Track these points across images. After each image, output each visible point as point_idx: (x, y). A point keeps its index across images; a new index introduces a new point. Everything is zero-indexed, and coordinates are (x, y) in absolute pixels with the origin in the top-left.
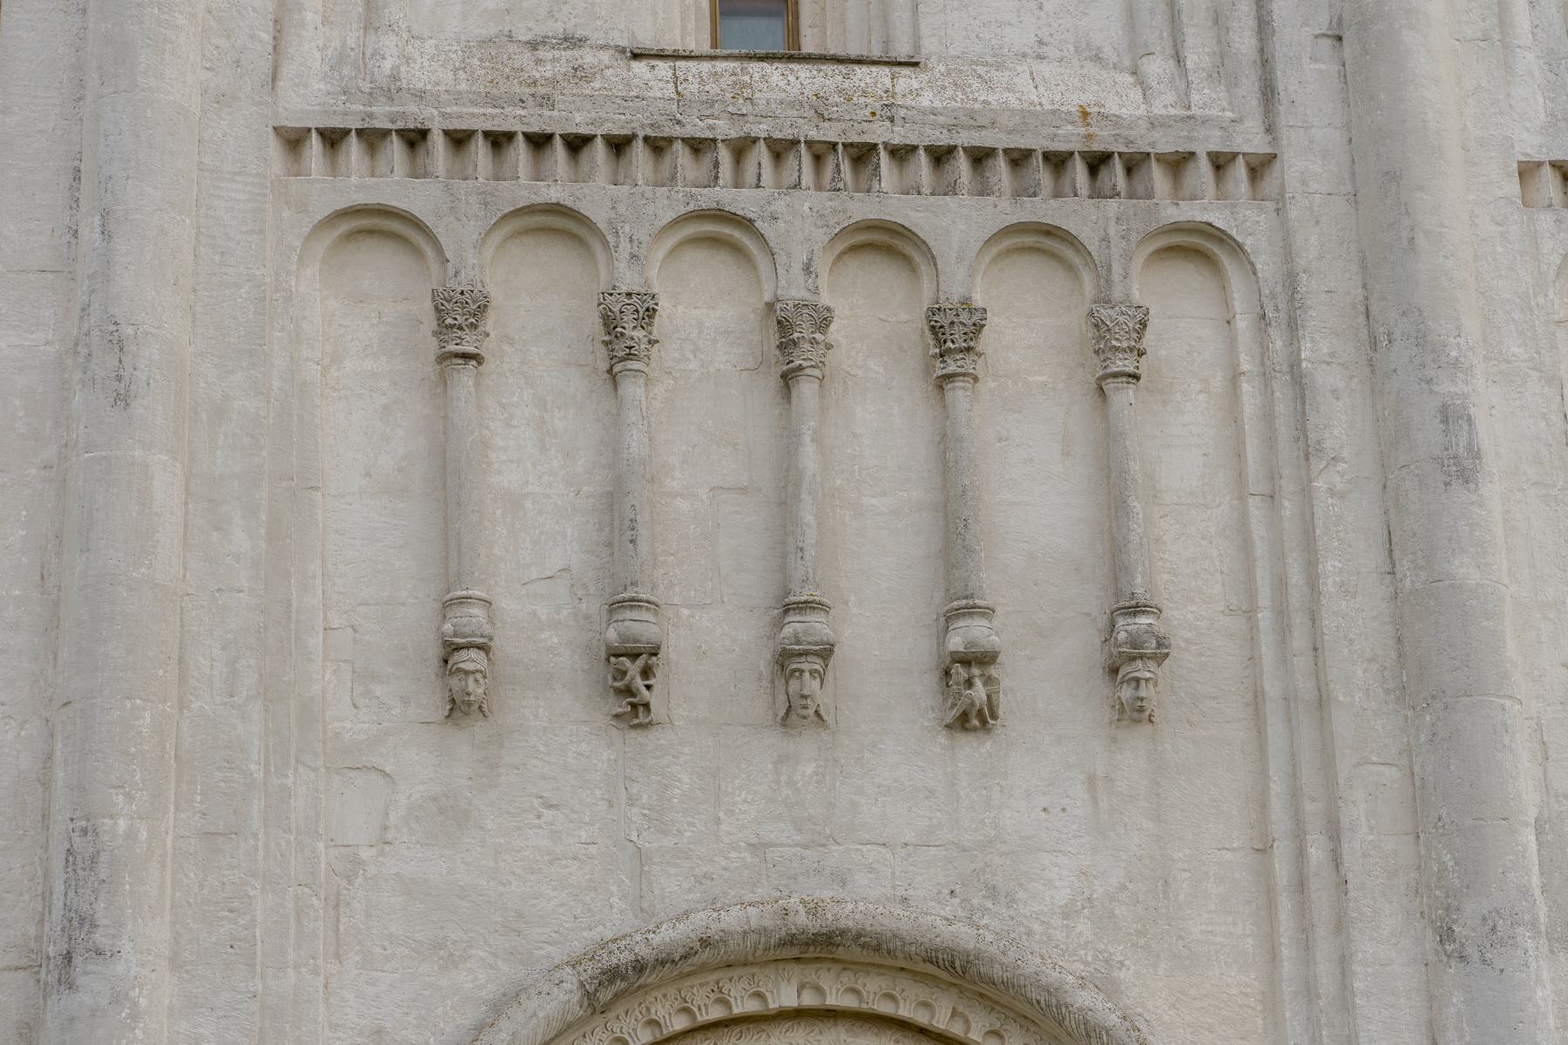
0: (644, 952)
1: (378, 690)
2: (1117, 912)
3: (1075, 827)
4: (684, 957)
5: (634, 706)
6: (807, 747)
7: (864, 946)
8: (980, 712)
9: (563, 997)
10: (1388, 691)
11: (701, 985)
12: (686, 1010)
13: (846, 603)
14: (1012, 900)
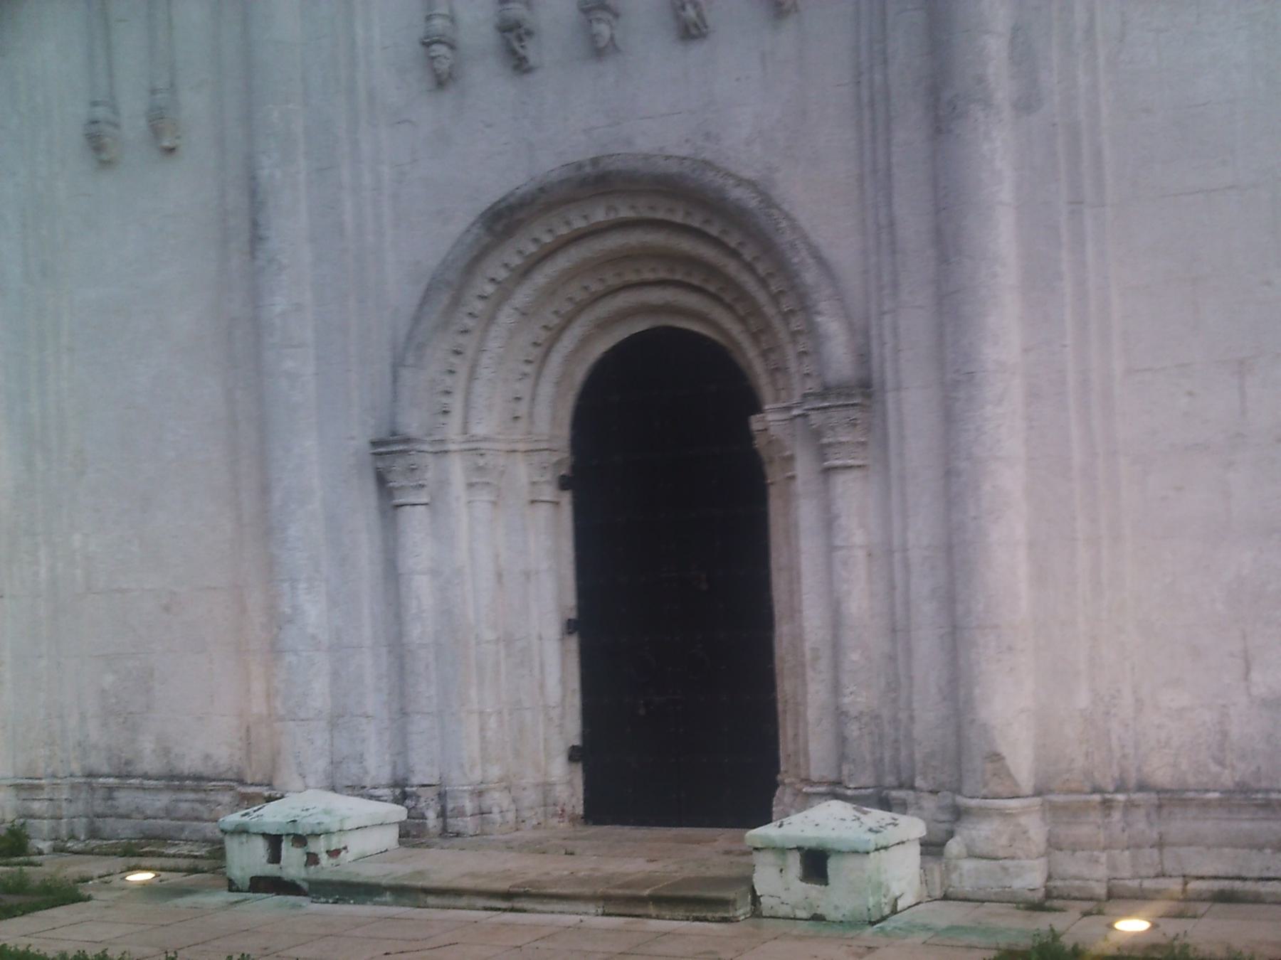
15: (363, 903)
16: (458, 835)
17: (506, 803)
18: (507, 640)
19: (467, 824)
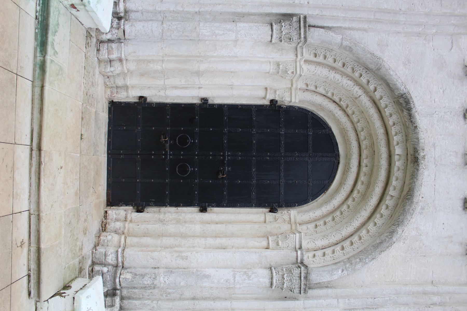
0: (414, 110)
4: (411, 122)
7: (414, 172)
9: (402, 88)
11: (401, 128)
14: (421, 213)
15: (36, 39)
16: (98, 50)
17: (117, 72)
18: (198, 74)
19: (104, 54)
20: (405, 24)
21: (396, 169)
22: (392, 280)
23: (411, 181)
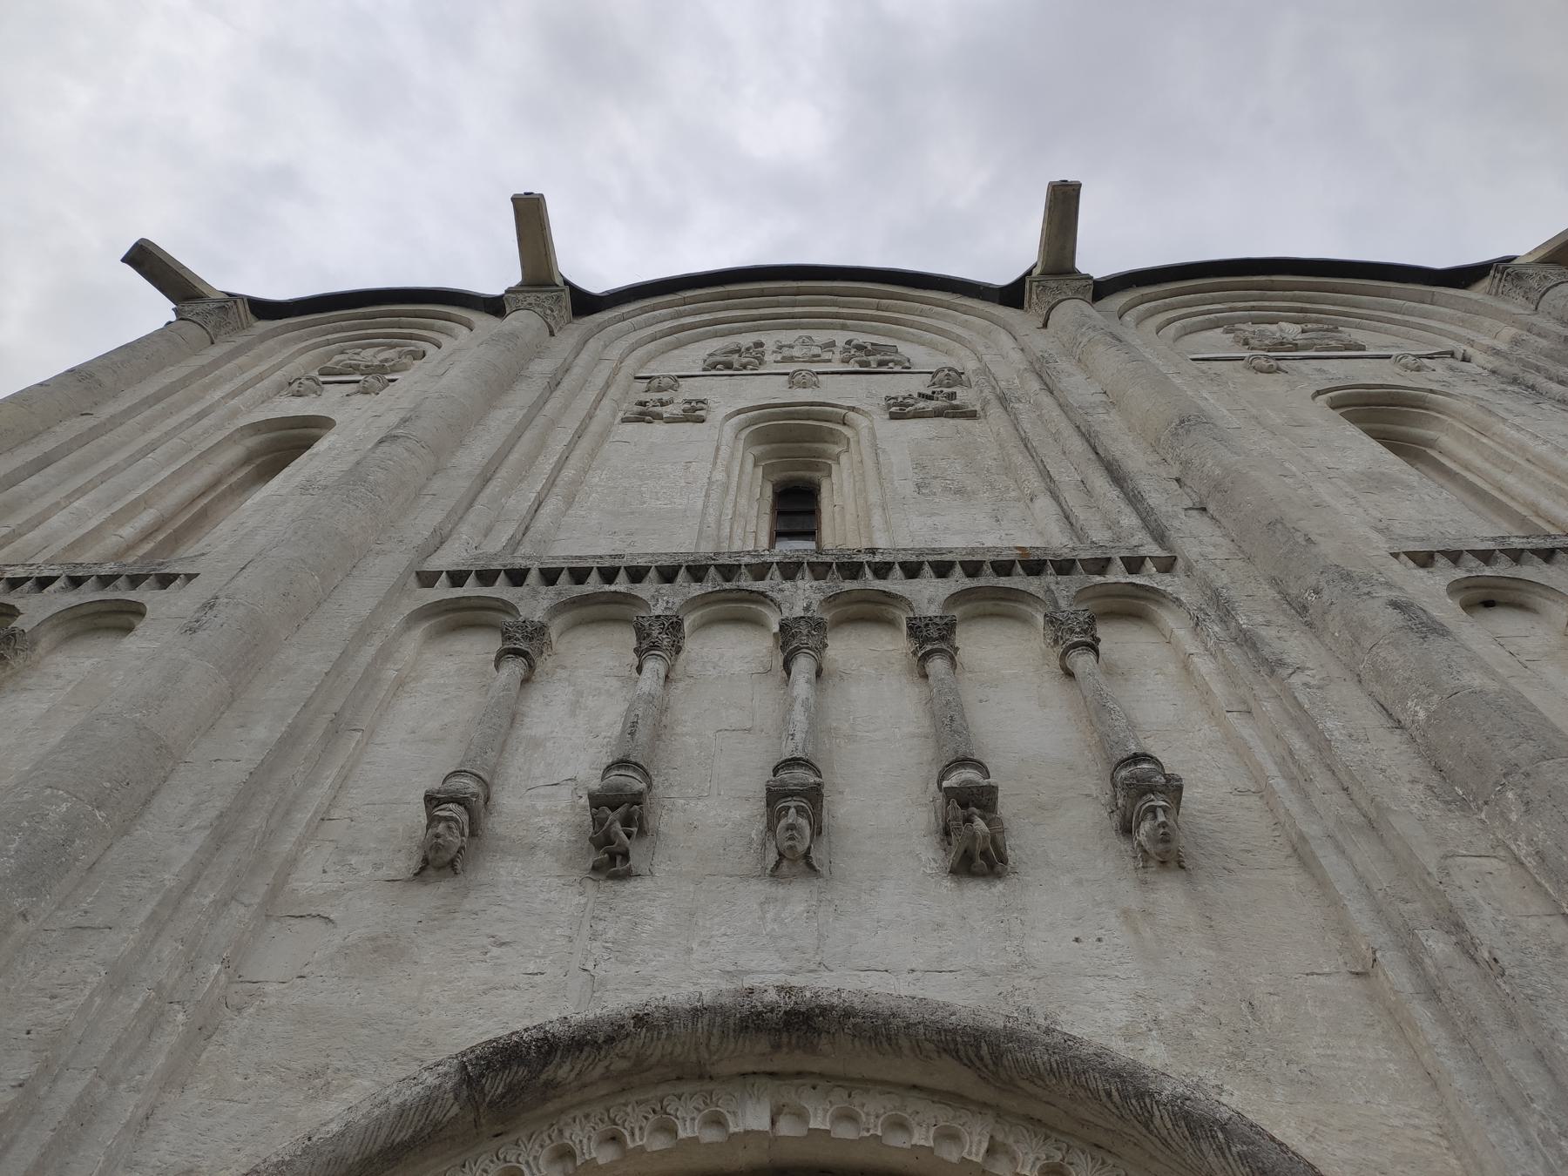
0: (558, 1029)
1: (353, 860)
2: (1196, 1033)
3: (1118, 954)
4: (610, 1040)
5: (612, 858)
6: (797, 897)
7: (857, 1033)
8: (984, 854)
9: (430, 1079)
10: (1447, 803)
12: (615, 1139)
13: (841, 793)
20: (114, 1083)
21: (845, 1132)
22: (1444, 1143)
23: (904, 1042)
